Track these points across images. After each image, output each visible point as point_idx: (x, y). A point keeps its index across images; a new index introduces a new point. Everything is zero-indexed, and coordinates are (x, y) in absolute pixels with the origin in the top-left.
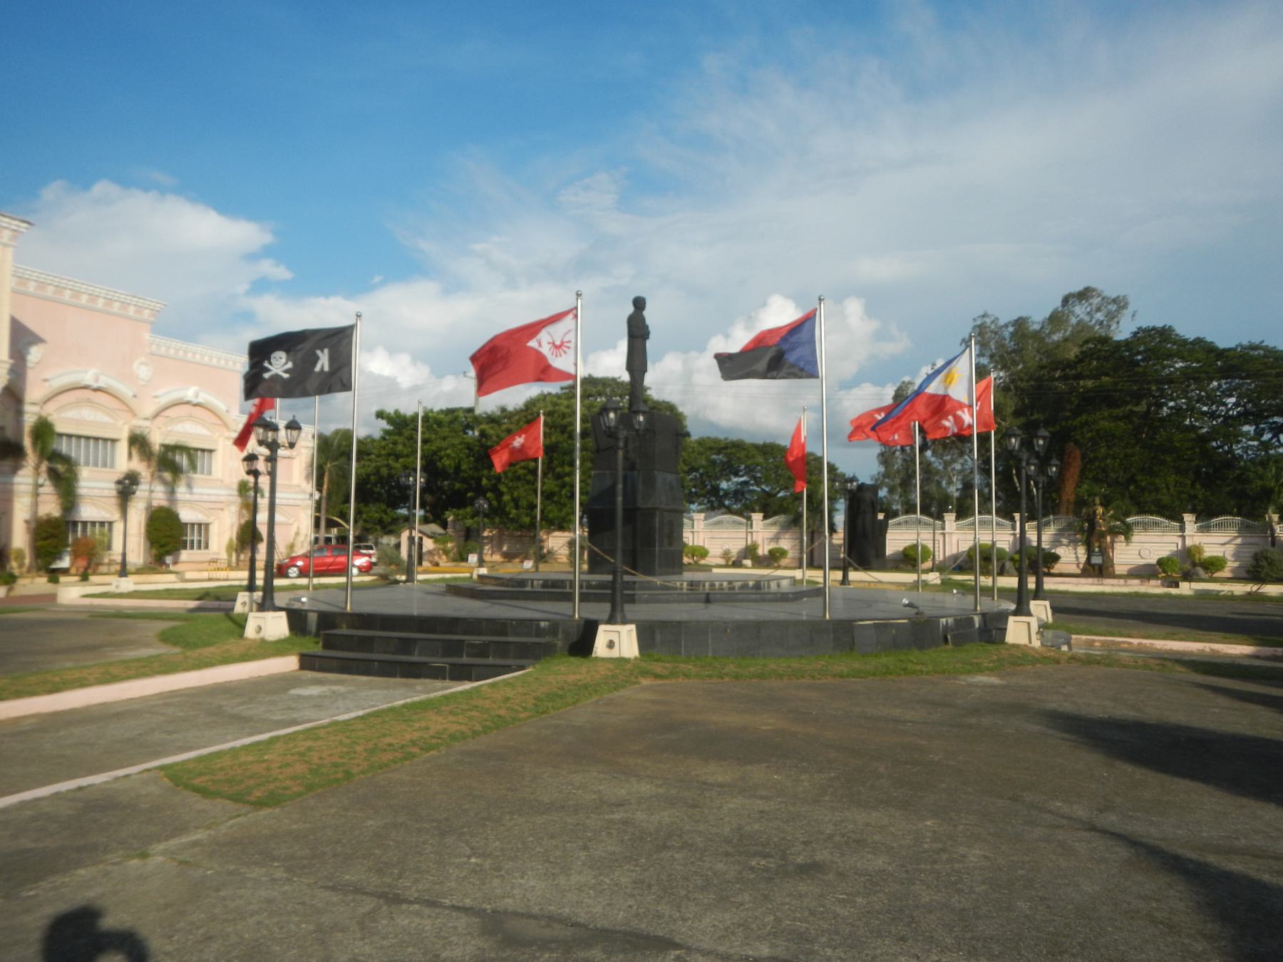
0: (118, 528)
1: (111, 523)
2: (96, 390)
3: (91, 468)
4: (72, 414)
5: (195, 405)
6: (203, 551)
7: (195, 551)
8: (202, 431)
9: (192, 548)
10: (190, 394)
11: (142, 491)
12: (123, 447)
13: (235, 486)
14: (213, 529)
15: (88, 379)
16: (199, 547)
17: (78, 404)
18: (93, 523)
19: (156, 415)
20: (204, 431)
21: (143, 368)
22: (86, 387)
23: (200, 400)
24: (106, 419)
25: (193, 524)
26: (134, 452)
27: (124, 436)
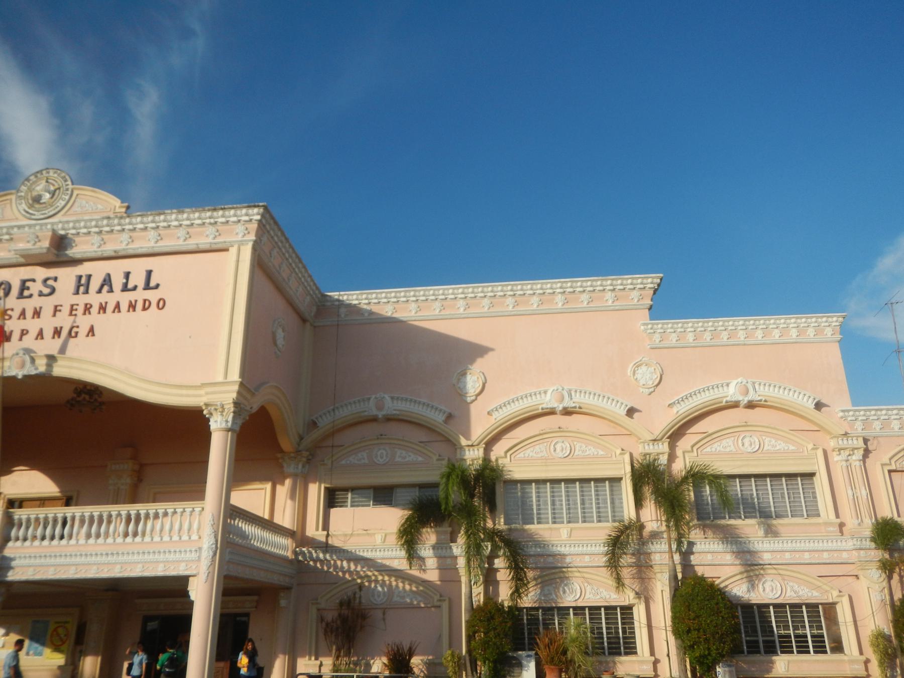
0: (639, 614)
1: (627, 610)
2: (567, 412)
3: (580, 525)
4: (529, 452)
5: (751, 405)
6: (829, 656)
7: (795, 657)
8: (770, 444)
9: (803, 649)
10: (732, 392)
11: (662, 555)
12: (627, 488)
13: (868, 532)
14: (843, 614)
15: (548, 400)
16: (820, 649)
17: (540, 436)
18: (595, 610)
19: (676, 435)
20: (781, 446)
21: (644, 368)
22: (552, 412)
23: (752, 396)
24: (591, 451)
25: (796, 607)
26: (647, 491)
27: (625, 471)
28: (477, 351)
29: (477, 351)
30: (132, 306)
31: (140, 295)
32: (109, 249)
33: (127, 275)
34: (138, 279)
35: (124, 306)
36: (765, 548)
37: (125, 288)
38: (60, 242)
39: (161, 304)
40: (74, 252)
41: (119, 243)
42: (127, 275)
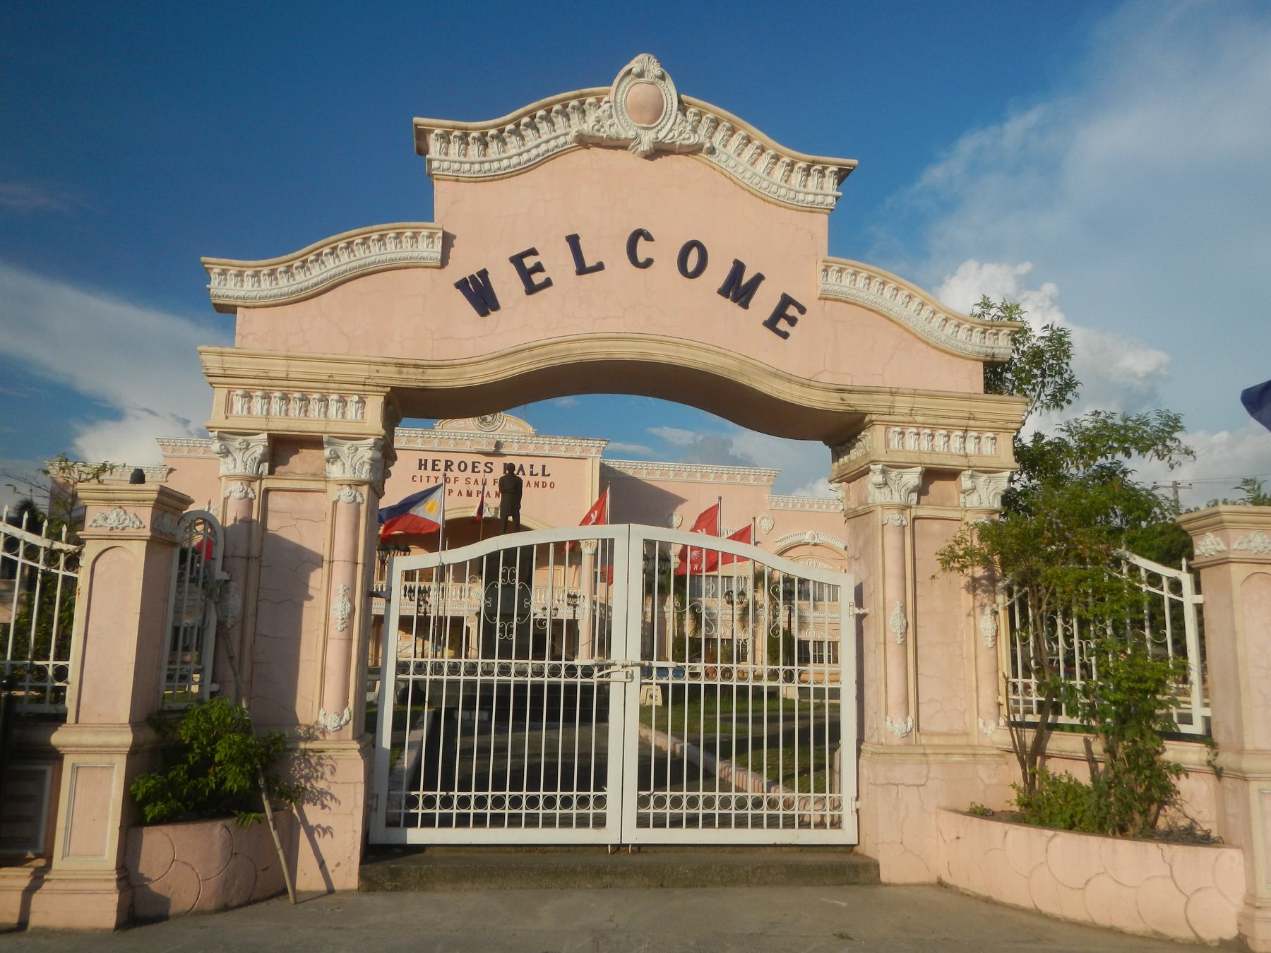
5: (815, 545)
10: (807, 538)
28: (681, 501)
29: (681, 501)
30: (537, 484)
31: (540, 479)
32: (524, 452)
33: (532, 466)
34: (538, 469)
35: (532, 484)
36: (811, 615)
37: (532, 474)
38: (498, 445)
39: (552, 485)
40: (502, 451)
41: (531, 449)
42: (532, 466)
